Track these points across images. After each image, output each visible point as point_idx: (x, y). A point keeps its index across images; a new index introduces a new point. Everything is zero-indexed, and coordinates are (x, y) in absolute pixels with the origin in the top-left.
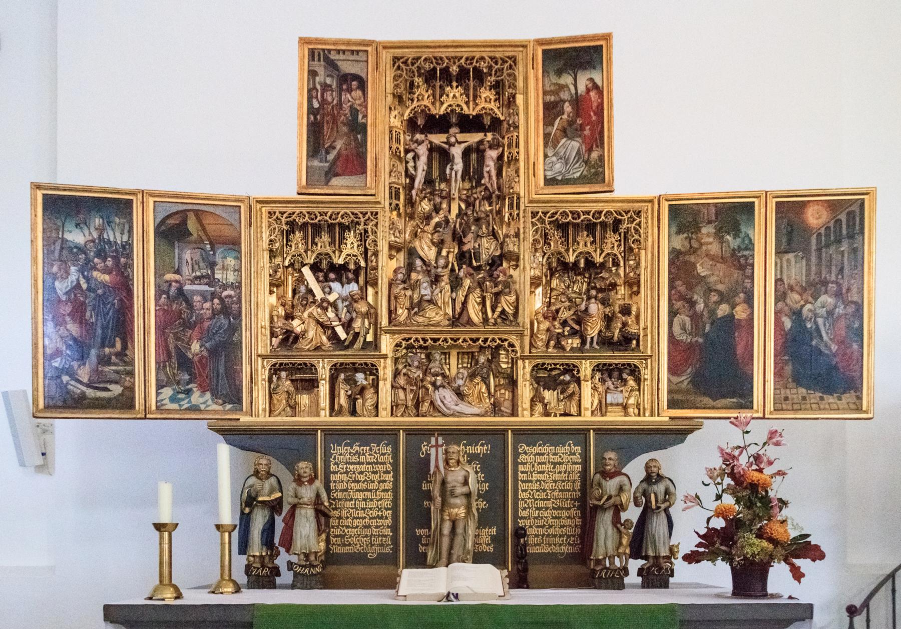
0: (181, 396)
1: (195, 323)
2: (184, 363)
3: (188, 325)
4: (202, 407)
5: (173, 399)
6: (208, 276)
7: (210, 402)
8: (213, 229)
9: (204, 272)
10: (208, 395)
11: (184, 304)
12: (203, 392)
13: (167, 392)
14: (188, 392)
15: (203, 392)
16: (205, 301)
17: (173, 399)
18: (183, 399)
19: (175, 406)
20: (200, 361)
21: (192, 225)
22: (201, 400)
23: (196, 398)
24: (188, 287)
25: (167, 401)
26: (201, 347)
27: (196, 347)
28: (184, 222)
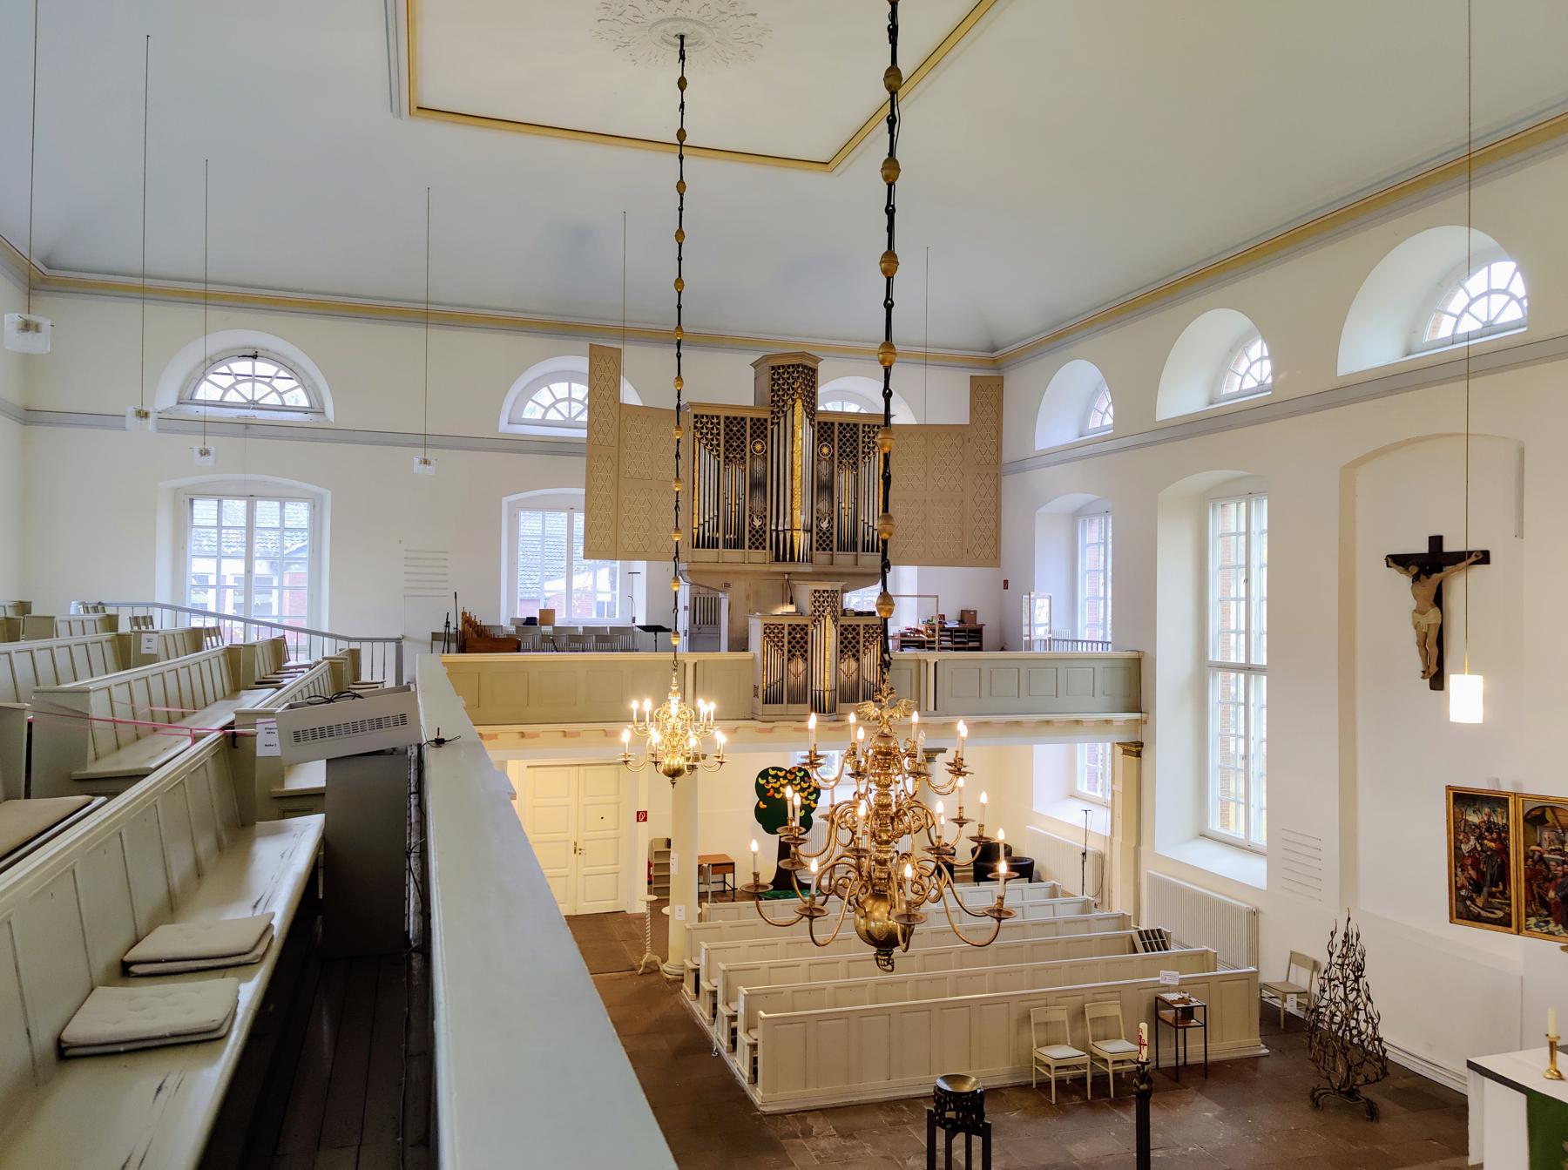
0: (1542, 924)
1: (1552, 879)
2: (1544, 903)
3: (1546, 879)
4: (1556, 933)
5: (1536, 925)
6: (1559, 850)
7: (1561, 931)
8: (1563, 820)
9: (1557, 847)
10: (1560, 927)
11: (1544, 866)
12: (1557, 924)
13: (1532, 920)
14: (1547, 923)
15: (1557, 924)
16: (1559, 866)
17: (1536, 925)
18: (1543, 926)
19: (1538, 930)
20: (1554, 904)
21: (1549, 815)
22: (1556, 929)
23: (1552, 927)
24: (1546, 856)
25: (1532, 926)
26: (1556, 894)
27: (1552, 894)
28: (1543, 814)
